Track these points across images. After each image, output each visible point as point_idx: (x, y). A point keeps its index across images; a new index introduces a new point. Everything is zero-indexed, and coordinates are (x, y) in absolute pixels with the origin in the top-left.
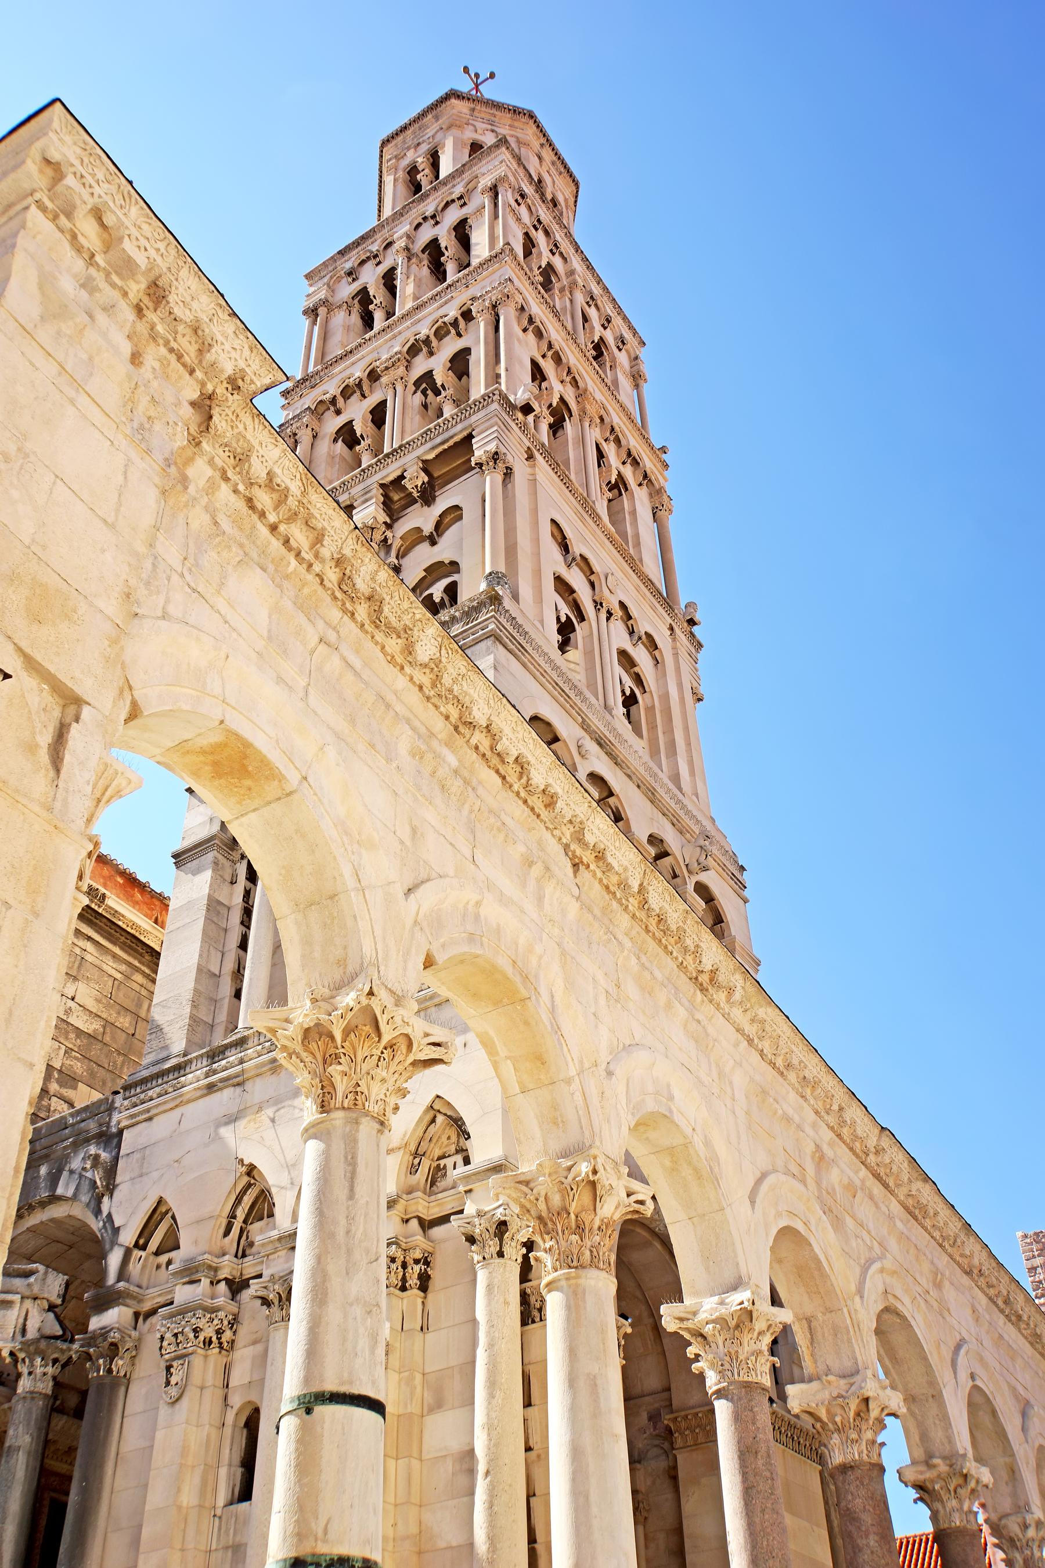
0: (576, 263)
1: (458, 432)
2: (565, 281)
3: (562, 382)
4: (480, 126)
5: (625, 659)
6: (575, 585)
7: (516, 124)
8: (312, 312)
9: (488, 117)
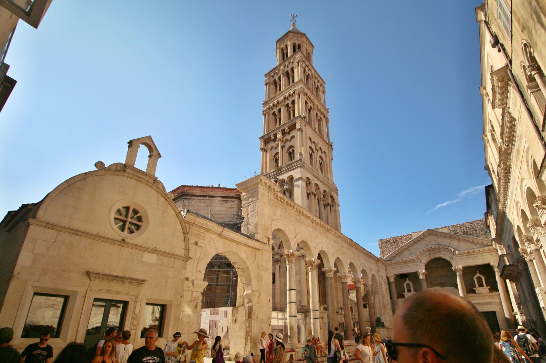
0: (313, 72)
1: (294, 122)
2: (311, 77)
3: (311, 103)
4: (295, 39)
5: (320, 157)
6: (312, 147)
7: (302, 37)
8: (266, 84)
9: (296, 36)
